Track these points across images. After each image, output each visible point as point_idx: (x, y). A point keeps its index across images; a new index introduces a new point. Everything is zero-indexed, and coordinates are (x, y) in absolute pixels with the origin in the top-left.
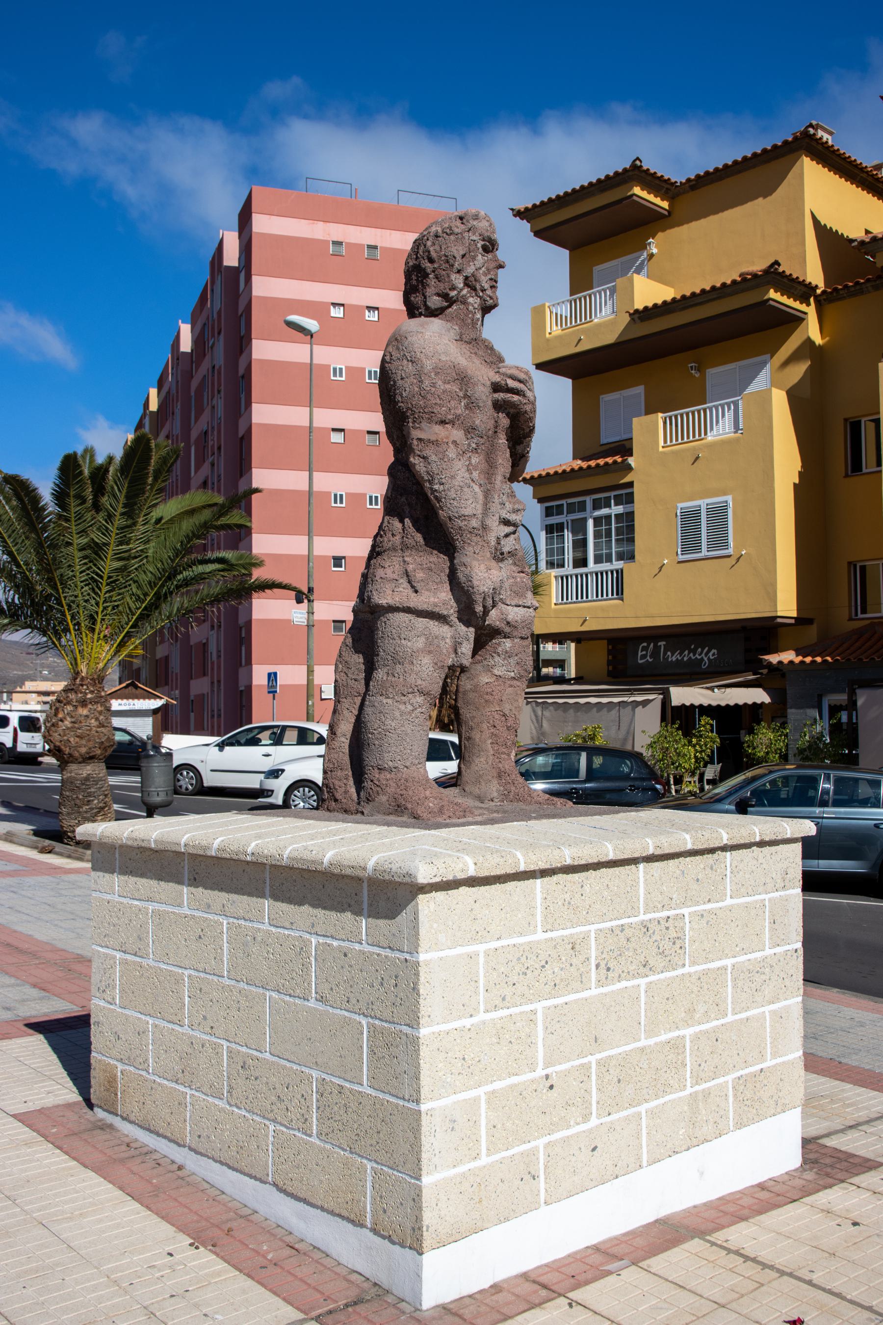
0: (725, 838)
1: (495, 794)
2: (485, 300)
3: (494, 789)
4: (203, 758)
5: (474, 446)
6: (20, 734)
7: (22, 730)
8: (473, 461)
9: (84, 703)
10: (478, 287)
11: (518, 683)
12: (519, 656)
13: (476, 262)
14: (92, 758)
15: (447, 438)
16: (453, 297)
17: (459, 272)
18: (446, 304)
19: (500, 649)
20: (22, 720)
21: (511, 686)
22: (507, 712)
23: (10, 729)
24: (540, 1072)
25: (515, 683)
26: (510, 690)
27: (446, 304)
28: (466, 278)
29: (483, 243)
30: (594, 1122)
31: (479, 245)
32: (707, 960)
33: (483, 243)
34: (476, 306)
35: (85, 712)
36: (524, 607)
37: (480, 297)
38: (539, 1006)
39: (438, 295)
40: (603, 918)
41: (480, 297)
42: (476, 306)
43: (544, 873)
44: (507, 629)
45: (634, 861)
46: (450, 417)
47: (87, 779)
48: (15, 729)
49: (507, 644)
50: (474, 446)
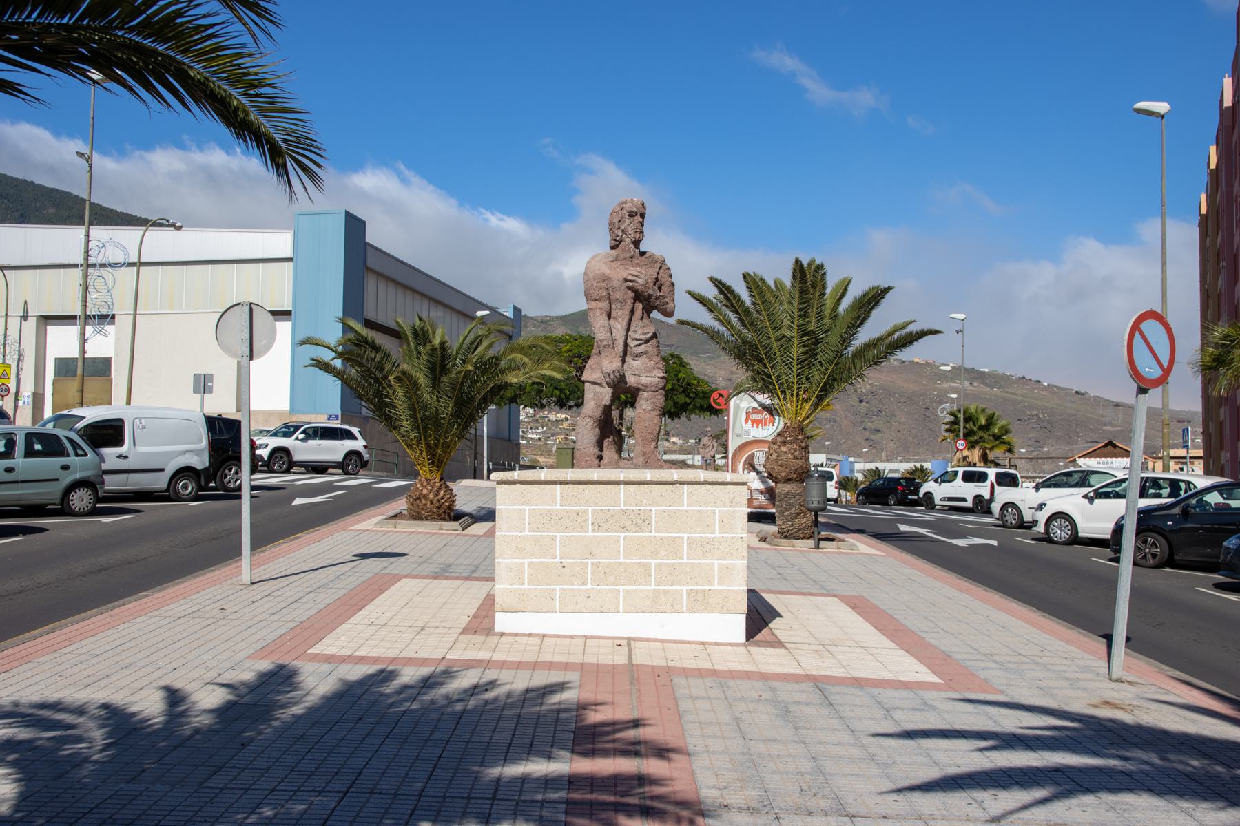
0: (676, 478)
4: (1021, 497)
6: (997, 488)
7: (999, 484)
9: (784, 443)
14: (790, 480)
20: (998, 476)
23: (988, 483)
24: (558, 559)
30: (589, 586)
32: (667, 532)
35: (784, 449)
38: (558, 535)
40: (596, 505)
43: (562, 483)
45: (618, 483)
47: (787, 494)
48: (992, 484)
49: (645, 394)
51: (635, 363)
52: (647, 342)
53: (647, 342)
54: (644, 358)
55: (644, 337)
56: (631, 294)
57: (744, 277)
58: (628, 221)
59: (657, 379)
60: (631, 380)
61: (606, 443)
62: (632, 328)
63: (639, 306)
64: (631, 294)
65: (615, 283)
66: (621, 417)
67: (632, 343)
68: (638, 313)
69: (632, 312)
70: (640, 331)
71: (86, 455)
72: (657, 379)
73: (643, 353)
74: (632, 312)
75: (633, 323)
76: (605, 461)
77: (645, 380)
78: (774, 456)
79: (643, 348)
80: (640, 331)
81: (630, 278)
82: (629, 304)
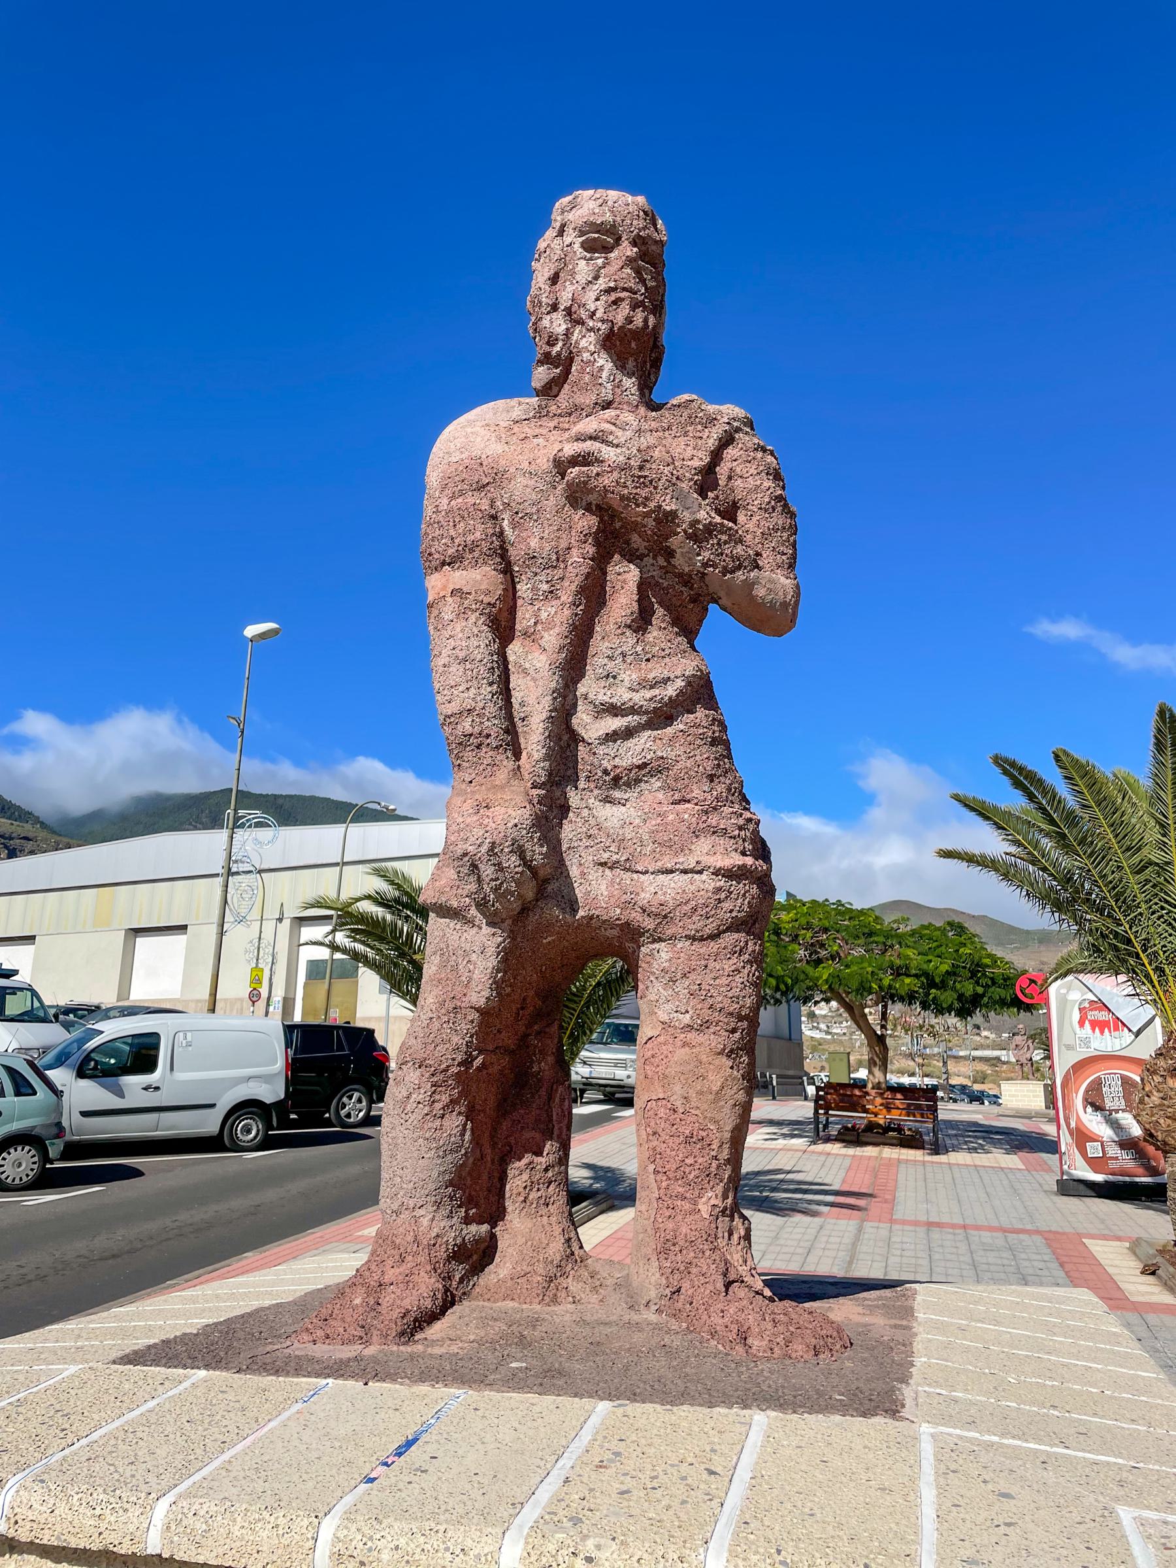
1: (653, 1294)
2: (599, 330)
3: (653, 1279)
5: (545, 587)
8: (544, 615)
10: (584, 314)
11: (701, 1038)
12: (692, 976)
13: (578, 278)
15: (444, 588)
16: (559, 354)
17: (554, 308)
18: (558, 371)
19: (655, 965)
21: (685, 1044)
22: (678, 1104)
25: (691, 1036)
26: (682, 1053)
27: (558, 371)
28: (569, 311)
29: (581, 239)
31: (577, 246)
33: (581, 239)
34: (592, 348)
36: (685, 872)
37: (591, 330)
39: (541, 363)
41: (591, 330)
42: (592, 348)
44: (649, 923)
46: (451, 551)
50: (545, 587)
51: (611, 815)
52: (662, 716)
53: (662, 716)
54: (653, 791)
55: (641, 698)
56: (586, 522)
57: (1057, 758)
58: (583, 270)
59: (707, 882)
60: (596, 890)
61: (517, 1178)
62: (597, 663)
63: (625, 578)
64: (586, 522)
65: (521, 488)
66: (884, 1016)
67: (590, 726)
68: (623, 599)
69: (594, 595)
70: (629, 676)
71: (35, 1093)
72: (707, 882)
73: (644, 770)
74: (594, 595)
75: (600, 646)
76: (500, 1270)
77: (657, 889)
78: (1155, 1098)
79: (642, 747)
80: (629, 676)
81: (570, 449)
82: (579, 560)
